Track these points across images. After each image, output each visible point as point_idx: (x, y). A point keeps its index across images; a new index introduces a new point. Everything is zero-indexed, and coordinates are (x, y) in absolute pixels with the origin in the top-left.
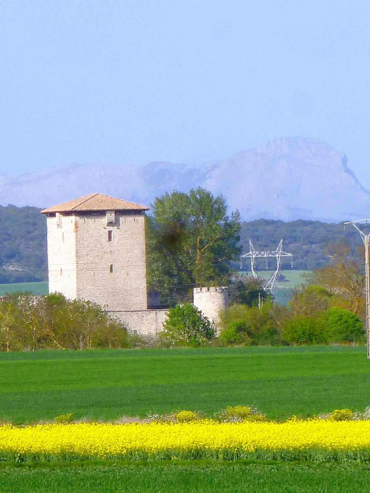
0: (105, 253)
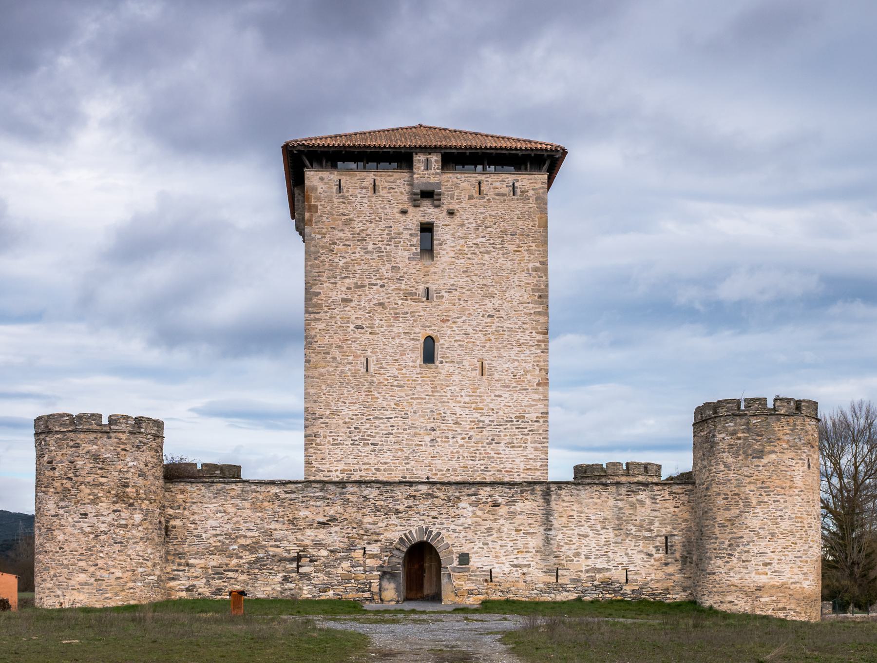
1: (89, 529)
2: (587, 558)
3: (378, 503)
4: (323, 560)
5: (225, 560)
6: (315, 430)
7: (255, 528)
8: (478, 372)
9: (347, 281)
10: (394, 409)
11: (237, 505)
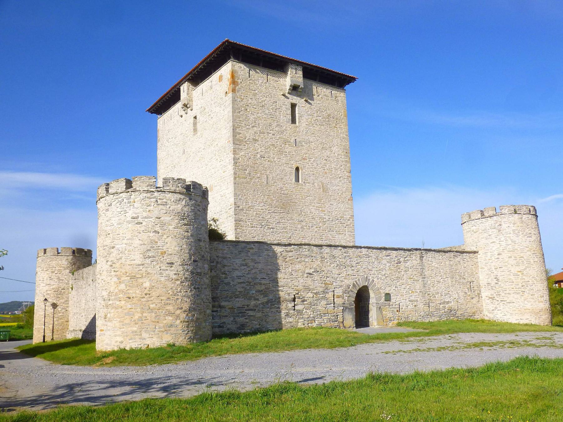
0: (286, 142)
1: (174, 277)
2: (442, 295)
3: (341, 260)
4: (311, 300)
5: (246, 302)
6: (241, 217)
7: (267, 278)
8: (322, 190)
9: (255, 128)
10: (282, 208)
11: (255, 260)
